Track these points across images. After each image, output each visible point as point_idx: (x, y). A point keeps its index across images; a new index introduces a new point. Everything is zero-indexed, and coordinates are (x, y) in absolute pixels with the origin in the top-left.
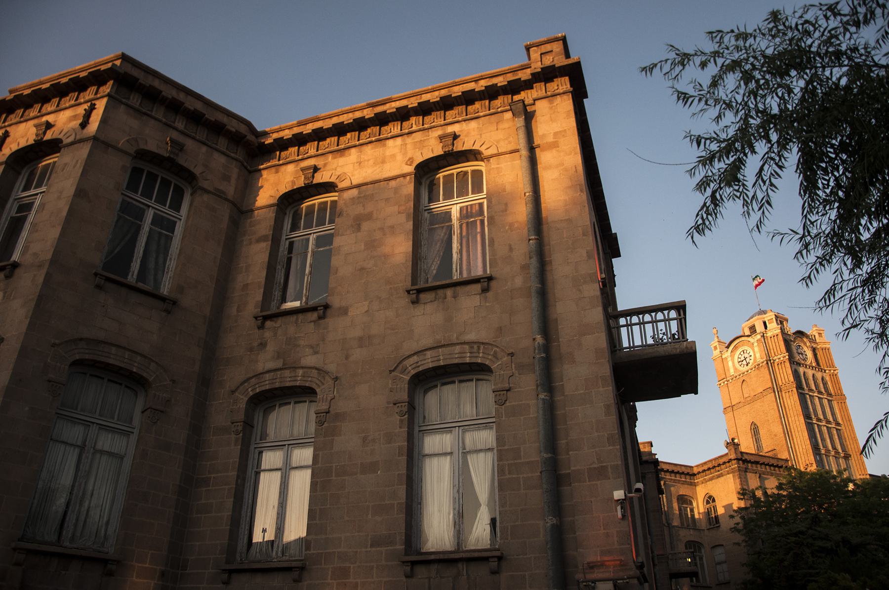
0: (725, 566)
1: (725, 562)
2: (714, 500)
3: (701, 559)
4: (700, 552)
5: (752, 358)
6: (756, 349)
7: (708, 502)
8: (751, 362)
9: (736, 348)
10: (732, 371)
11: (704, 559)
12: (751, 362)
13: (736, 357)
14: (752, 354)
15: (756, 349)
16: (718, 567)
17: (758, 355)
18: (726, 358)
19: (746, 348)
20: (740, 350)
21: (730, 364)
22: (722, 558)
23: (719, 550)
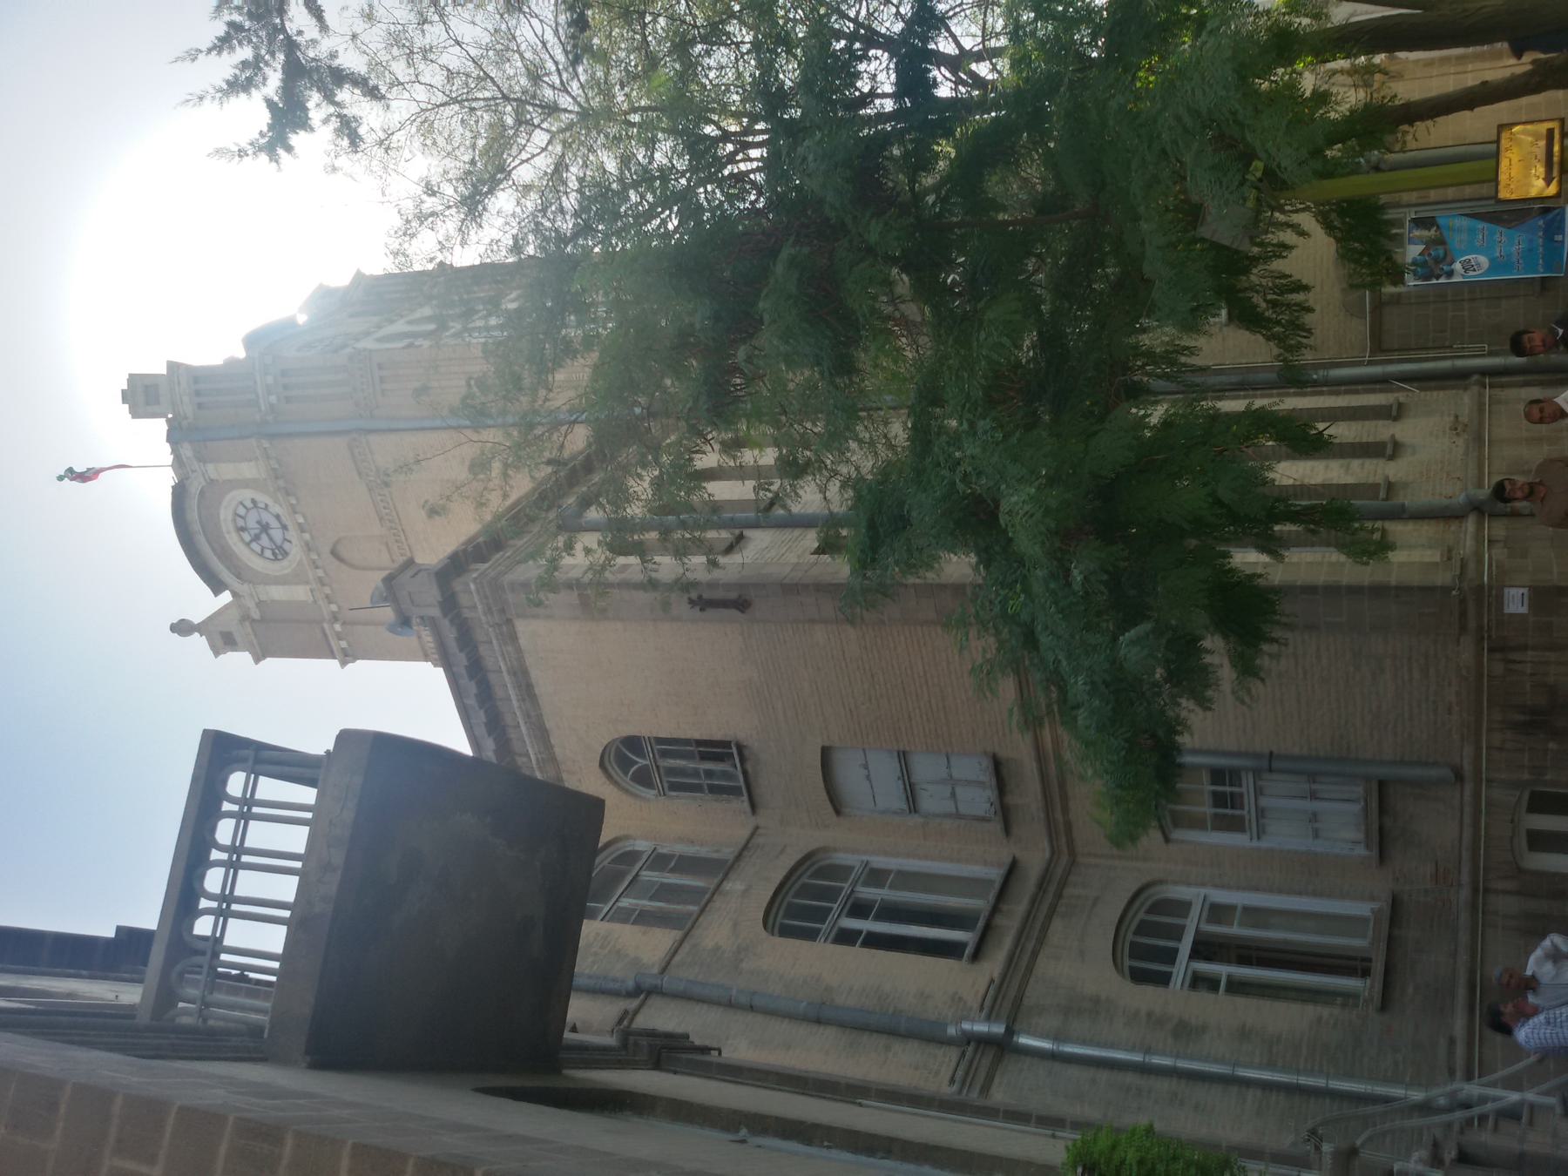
0: (925, 768)
1: (903, 757)
2: (633, 743)
3: (876, 877)
4: (842, 872)
5: (262, 499)
6: (226, 471)
7: (643, 778)
8: (270, 502)
9: (226, 556)
10: (300, 593)
11: (879, 862)
12: (277, 509)
13: (257, 564)
14: (247, 495)
15: (226, 471)
16: (927, 803)
17: (248, 470)
18: (260, 604)
19: (225, 515)
20: (233, 540)
21: (277, 593)
22: (885, 768)
23: (850, 775)
